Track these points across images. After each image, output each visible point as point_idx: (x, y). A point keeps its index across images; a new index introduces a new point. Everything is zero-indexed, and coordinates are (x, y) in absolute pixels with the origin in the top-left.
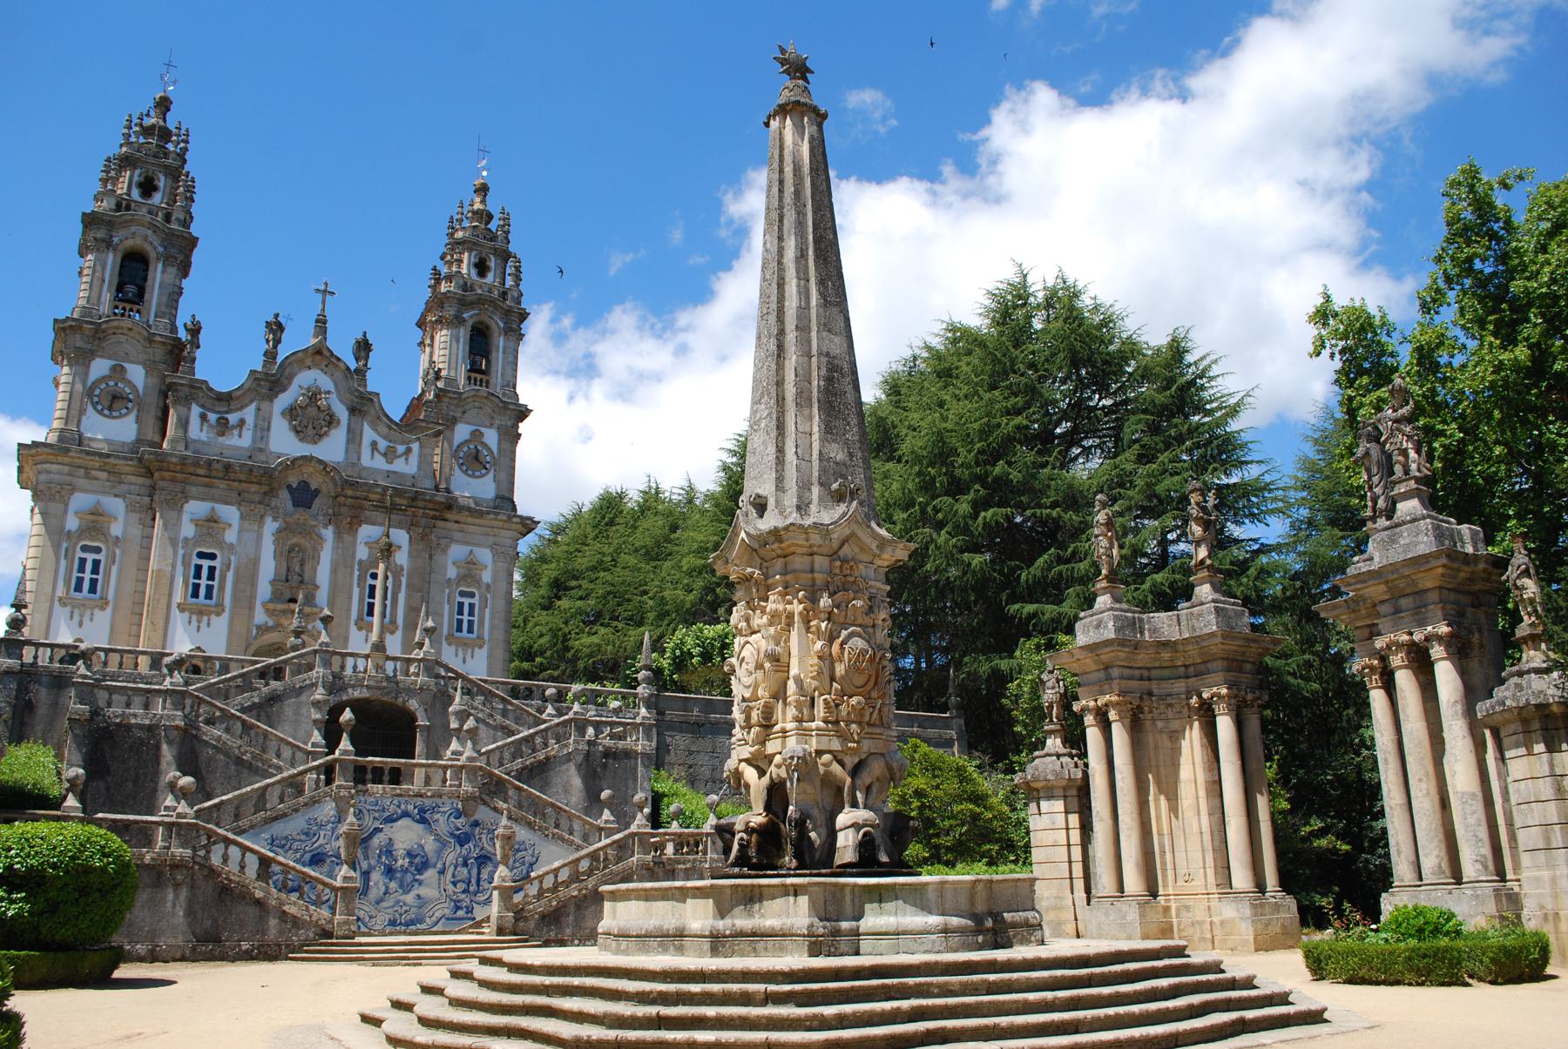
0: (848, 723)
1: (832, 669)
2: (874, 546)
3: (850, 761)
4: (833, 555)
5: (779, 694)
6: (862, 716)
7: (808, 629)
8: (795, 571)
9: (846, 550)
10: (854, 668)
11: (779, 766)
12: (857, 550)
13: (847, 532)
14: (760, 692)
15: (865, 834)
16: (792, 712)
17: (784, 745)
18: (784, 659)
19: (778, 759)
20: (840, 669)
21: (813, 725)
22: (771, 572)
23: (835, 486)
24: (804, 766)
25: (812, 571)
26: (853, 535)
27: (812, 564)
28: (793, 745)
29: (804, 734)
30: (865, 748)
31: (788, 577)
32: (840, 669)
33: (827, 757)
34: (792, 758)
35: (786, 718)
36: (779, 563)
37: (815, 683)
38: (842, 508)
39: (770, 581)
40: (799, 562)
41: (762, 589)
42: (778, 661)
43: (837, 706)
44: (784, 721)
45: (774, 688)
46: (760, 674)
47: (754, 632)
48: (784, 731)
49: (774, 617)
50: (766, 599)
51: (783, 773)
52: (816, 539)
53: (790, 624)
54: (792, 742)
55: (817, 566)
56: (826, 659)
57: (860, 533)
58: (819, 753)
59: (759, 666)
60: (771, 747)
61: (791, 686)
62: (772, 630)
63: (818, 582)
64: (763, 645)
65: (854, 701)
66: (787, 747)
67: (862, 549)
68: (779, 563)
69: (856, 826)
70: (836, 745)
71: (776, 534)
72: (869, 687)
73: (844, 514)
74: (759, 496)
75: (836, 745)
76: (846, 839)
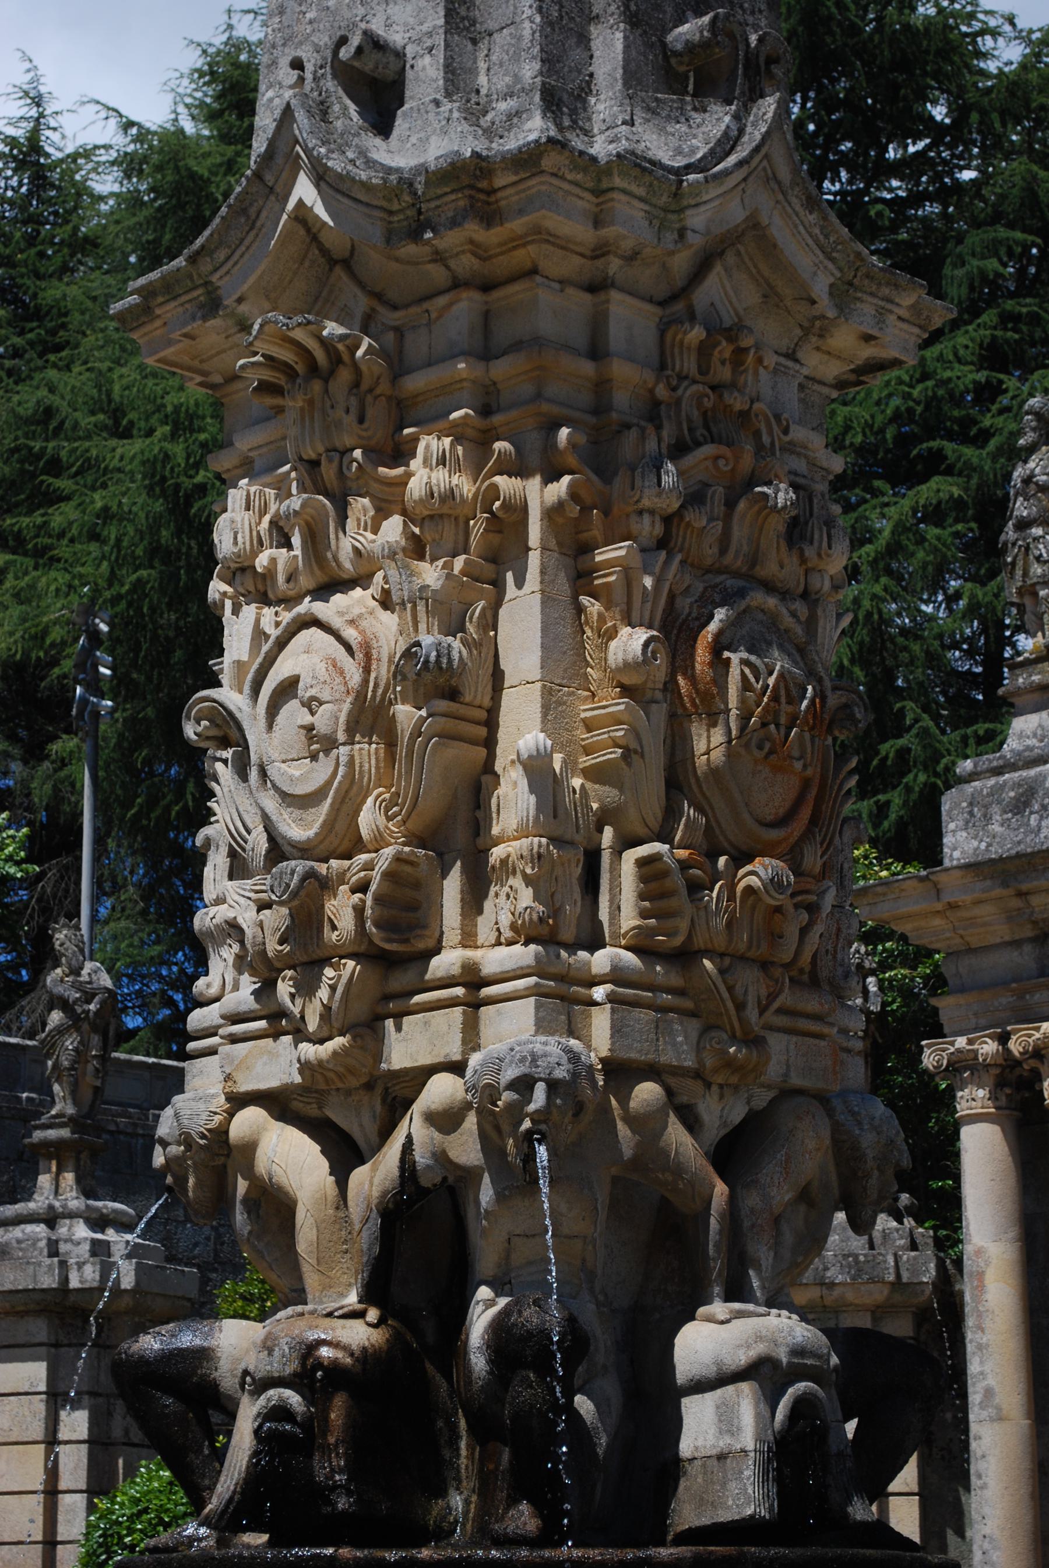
0: (730, 960)
1: (677, 746)
2: (820, 287)
3: (722, 1113)
4: (675, 300)
5: (455, 832)
6: (775, 937)
7: (582, 578)
8: (536, 343)
9: (713, 289)
10: (759, 741)
11: (446, 1120)
12: (751, 296)
13: (736, 214)
14: (369, 818)
15: (800, 1405)
16: (512, 901)
17: (471, 1037)
18: (476, 691)
19: (442, 1089)
20: (709, 744)
21: (601, 960)
22: (417, 345)
23: (689, 30)
24: (558, 1121)
25: (597, 352)
26: (753, 227)
27: (598, 324)
28: (513, 1029)
29: (562, 998)
30: (774, 1070)
31: (501, 369)
32: (709, 744)
33: (647, 1092)
34: (524, 1085)
35: (485, 937)
36: (462, 311)
37: (599, 797)
38: (717, 120)
39: (416, 383)
40: (552, 310)
41: (376, 411)
42: (456, 693)
43: (695, 888)
44: (468, 939)
45: (432, 804)
46: (367, 753)
47: (345, 585)
48: (473, 980)
49: (433, 527)
50: (400, 453)
51: (466, 1147)
52: (631, 220)
53: (502, 554)
54: (513, 1029)
55: (616, 334)
56: (666, 698)
57: (779, 229)
58: (621, 1072)
59: (369, 717)
60: (406, 1046)
61: (514, 801)
62: (430, 574)
63: (621, 399)
64: (387, 631)
65: (757, 873)
66: (489, 1032)
67: (770, 295)
68: (462, 311)
69: (764, 1373)
70: (679, 1047)
71: (469, 181)
72: (798, 827)
73: (727, 143)
74: (374, 43)
75: (679, 1047)
76: (727, 1421)
